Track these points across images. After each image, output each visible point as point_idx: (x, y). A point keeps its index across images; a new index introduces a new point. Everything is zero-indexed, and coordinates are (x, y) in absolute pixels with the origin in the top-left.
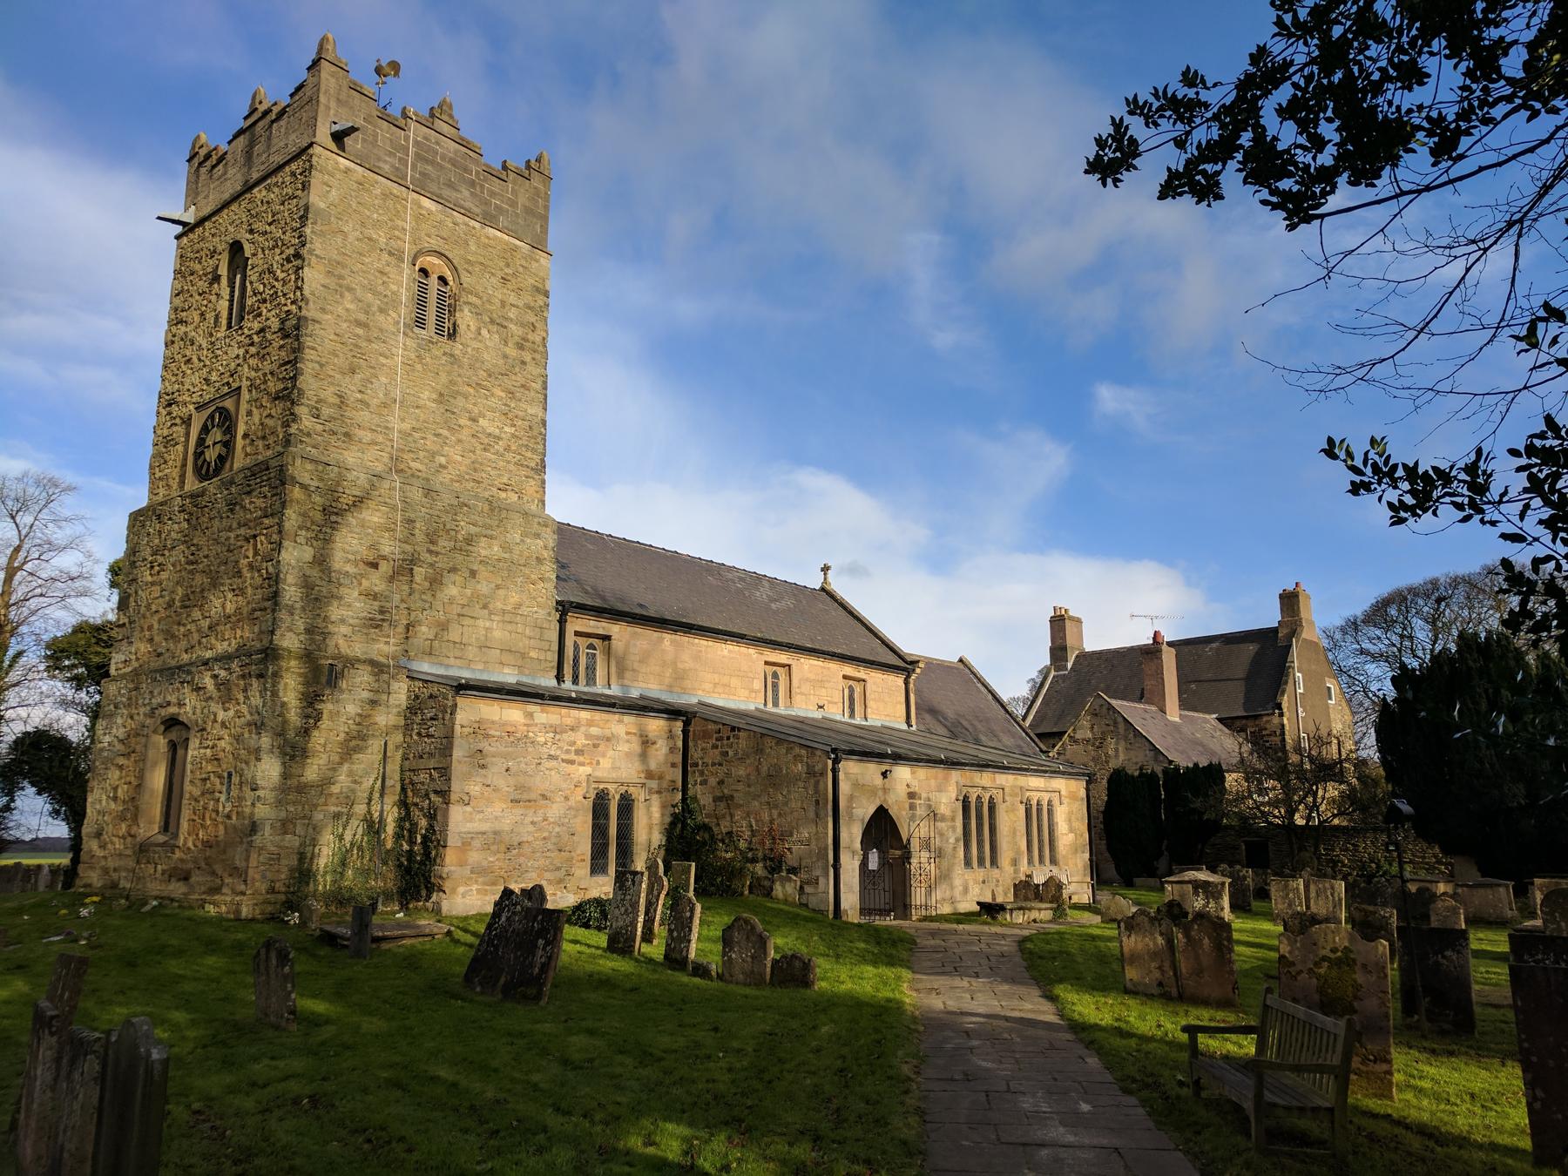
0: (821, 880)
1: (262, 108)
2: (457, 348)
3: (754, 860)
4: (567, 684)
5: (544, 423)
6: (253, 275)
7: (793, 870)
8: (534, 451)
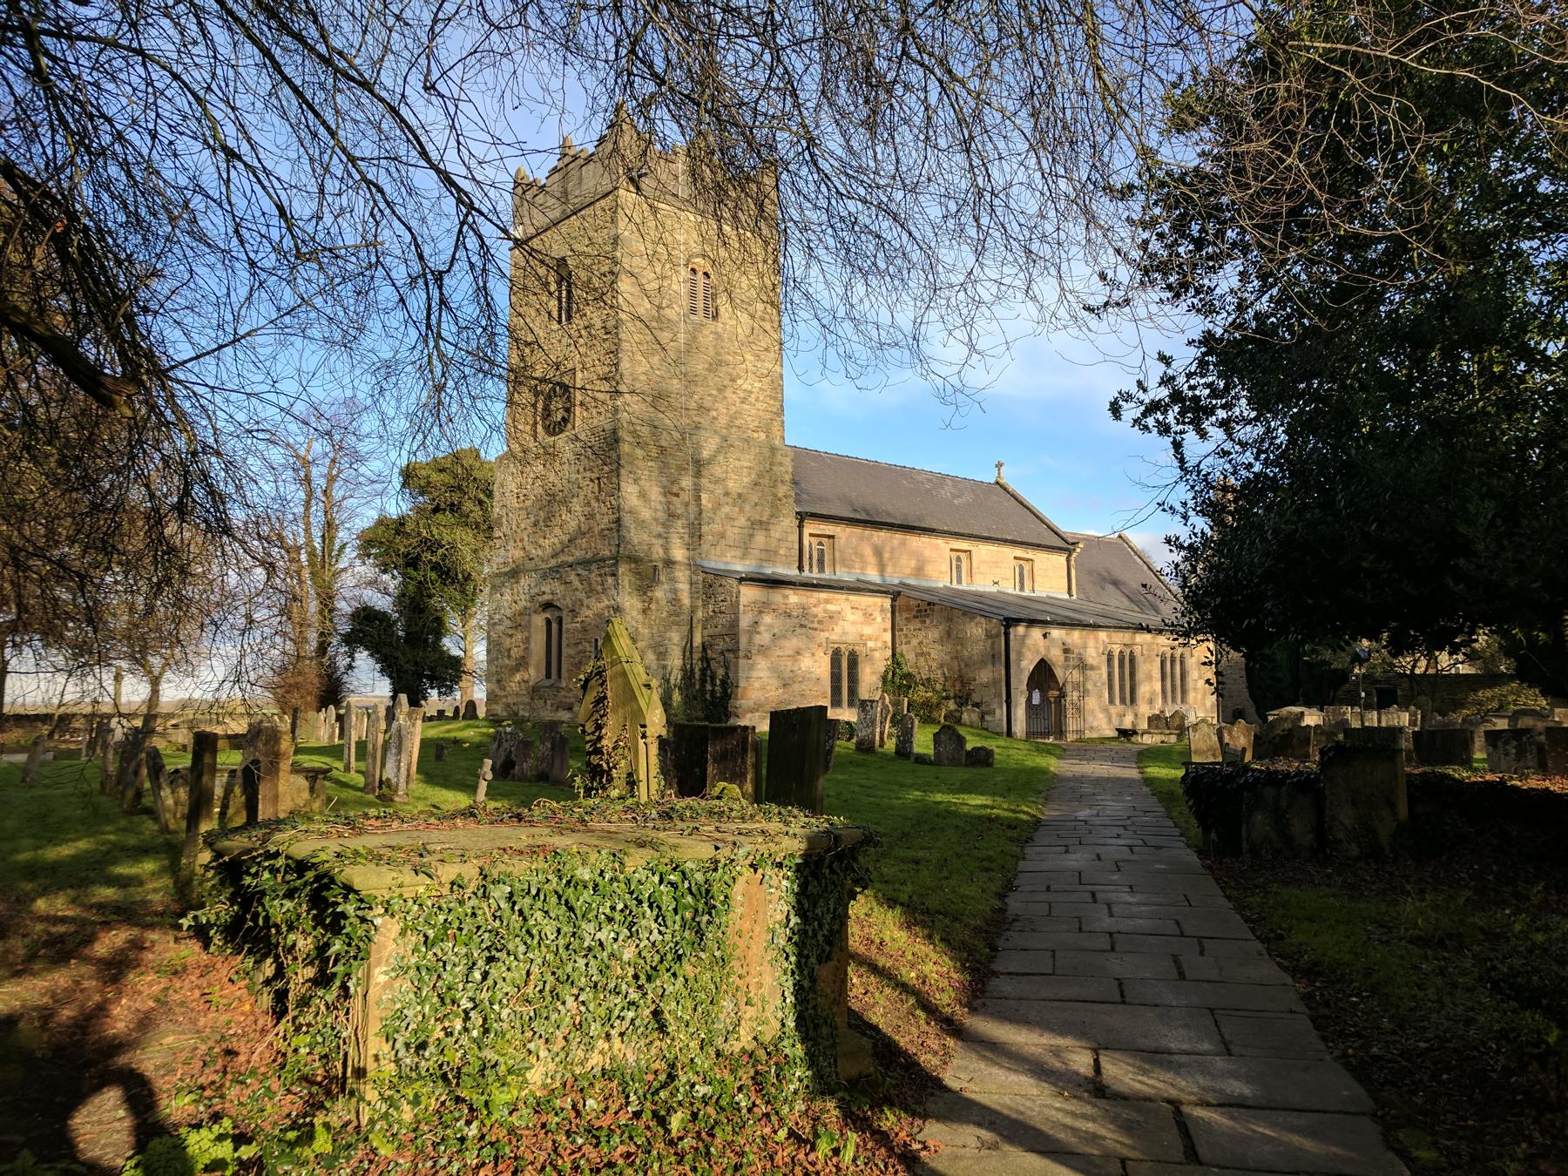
3: (947, 698)
4: (806, 573)
5: (781, 376)
7: (977, 705)
8: (775, 399)
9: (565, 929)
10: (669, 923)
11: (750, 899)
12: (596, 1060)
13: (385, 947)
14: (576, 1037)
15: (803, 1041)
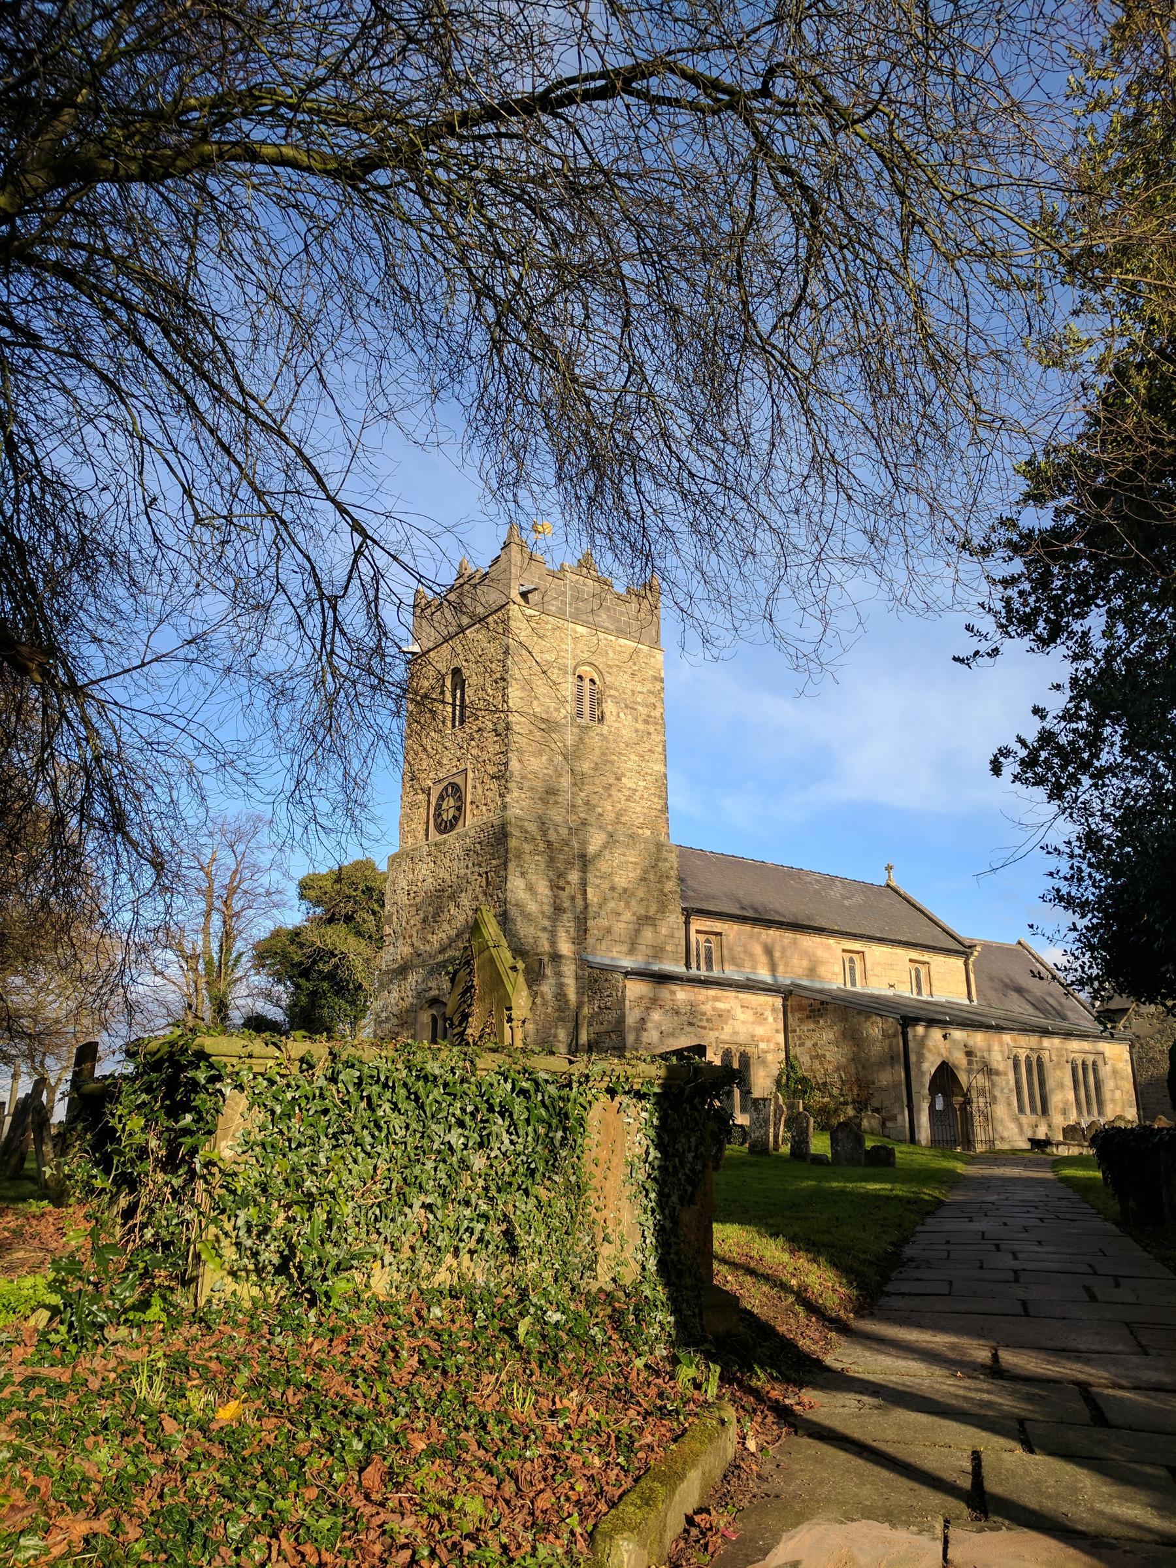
0: (899, 1118)
1: (468, 572)
2: (605, 729)
3: (845, 1103)
5: (665, 776)
6: (469, 692)
8: (660, 797)
9: (414, 1125)
10: (521, 1133)
11: (607, 1125)
12: (443, 1277)
13: (232, 1120)
14: (423, 1249)
15: (666, 1285)
